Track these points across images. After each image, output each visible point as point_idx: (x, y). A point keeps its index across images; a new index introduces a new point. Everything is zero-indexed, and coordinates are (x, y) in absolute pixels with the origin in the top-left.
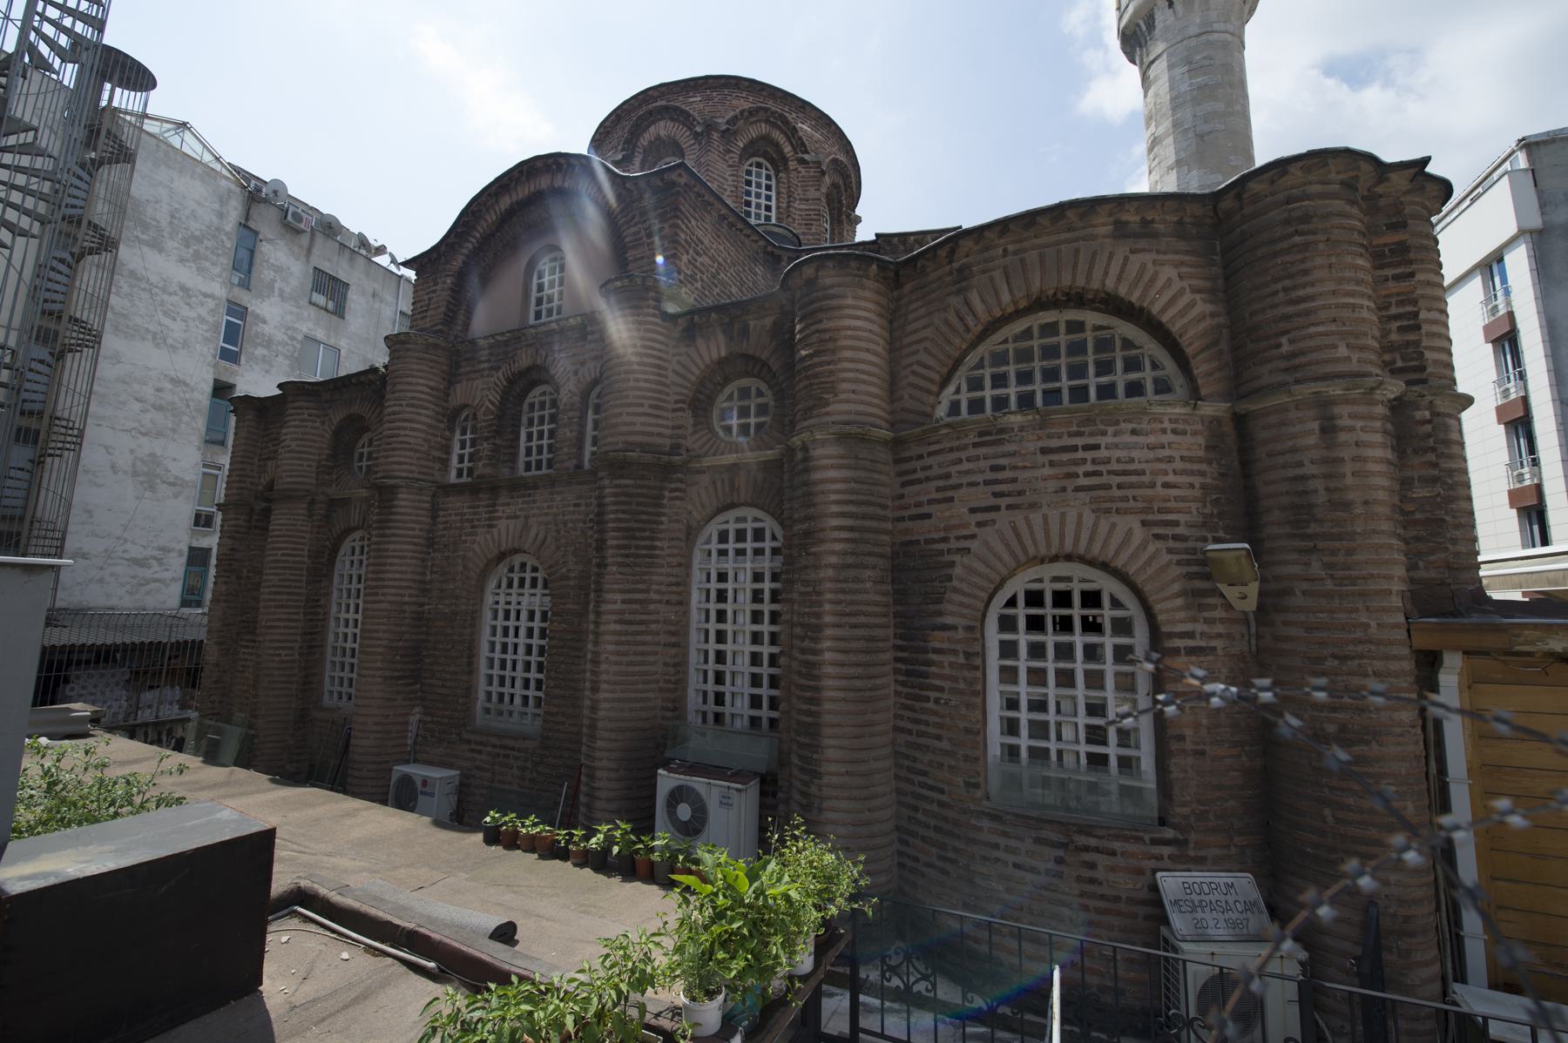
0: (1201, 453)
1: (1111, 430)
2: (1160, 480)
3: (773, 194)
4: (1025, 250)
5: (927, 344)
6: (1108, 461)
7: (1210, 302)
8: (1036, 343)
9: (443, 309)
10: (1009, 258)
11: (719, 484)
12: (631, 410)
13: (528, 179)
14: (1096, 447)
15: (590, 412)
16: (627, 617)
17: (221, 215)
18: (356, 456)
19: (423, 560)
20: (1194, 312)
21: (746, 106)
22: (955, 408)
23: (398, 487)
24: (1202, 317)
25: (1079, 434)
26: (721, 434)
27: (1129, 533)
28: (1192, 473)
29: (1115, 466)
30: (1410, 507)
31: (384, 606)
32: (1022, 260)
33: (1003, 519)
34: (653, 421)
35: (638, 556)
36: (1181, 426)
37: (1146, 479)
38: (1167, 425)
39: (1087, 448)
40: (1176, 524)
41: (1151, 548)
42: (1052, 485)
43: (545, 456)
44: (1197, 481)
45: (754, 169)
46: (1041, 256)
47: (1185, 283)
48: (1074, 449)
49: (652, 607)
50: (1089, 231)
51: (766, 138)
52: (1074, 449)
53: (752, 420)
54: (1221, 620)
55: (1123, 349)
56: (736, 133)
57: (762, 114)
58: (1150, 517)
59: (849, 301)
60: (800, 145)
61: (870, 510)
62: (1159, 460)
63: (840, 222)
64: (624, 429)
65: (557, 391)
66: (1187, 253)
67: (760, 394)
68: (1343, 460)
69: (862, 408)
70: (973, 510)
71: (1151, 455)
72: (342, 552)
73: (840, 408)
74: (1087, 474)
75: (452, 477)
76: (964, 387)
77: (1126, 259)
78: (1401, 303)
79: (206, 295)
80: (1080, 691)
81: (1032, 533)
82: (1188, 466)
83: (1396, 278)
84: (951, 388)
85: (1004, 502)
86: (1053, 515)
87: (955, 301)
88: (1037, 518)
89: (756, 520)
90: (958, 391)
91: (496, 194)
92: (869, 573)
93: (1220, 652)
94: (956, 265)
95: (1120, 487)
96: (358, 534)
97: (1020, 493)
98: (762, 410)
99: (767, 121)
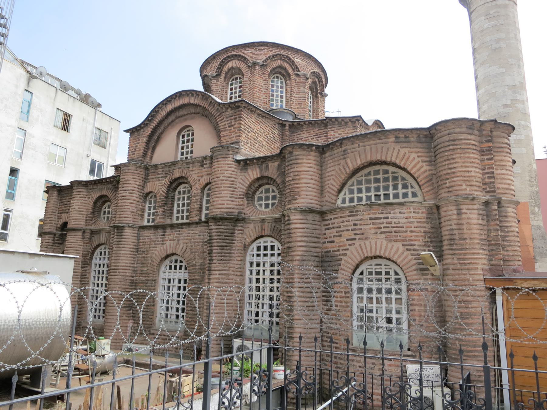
0: (425, 220)
1: (392, 212)
2: (409, 230)
3: (284, 90)
4: (365, 146)
5: (334, 177)
7: (429, 165)
9: (142, 151)
10: (360, 148)
11: (257, 228)
12: (222, 199)
13: (179, 99)
14: (387, 218)
15: (205, 197)
16: (221, 280)
17: (17, 86)
18: (102, 212)
19: (134, 258)
20: (422, 170)
22: (344, 201)
23: (123, 227)
24: (426, 171)
25: (382, 213)
26: (258, 207)
27: (398, 249)
28: (420, 227)
29: (393, 225)
30: (490, 239)
31: (119, 277)
32: (365, 149)
33: (357, 243)
34: (231, 203)
35: (225, 257)
36: (417, 211)
37: (404, 229)
38: (412, 210)
39: (385, 218)
40: (414, 245)
41: (405, 254)
42: (373, 231)
43: (185, 214)
44: (423, 230)
45: (275, 79)
46: (371, 149)
47: (420, 159)
48: (380, 218)
49: (231, 277)
50: (387, 140)
51: (281, 67)
52: (380, 218)
53: (270, 202)
54: (430, 279)
55: (401, 181)
56: (266, 65)
57: (279, 57)
58: (405, 243)
59: (305, 161)
60: (296, 68)
61: (313, 239)
62: (409, 223)
63: (317, 97)
64: (220, 206)
65: (191, 187)
66: (420, 148)
67: (273, 191)
68: (463, 224)
69: (309, 201)
70: (348, 240)
71: (406, 221)
72: (95, 254)
74: (384, 227)
75: (145, 223)
76: (347, 193)
77: (399, 150)
78: (489, 168)
79: (9, 126)
80: (384, 305)
81: (366, 248)
82: (419, 225)
83: (488, 159)
84: (342, 193)
85: (357, 237)
86: (373, 242)
87: (342, 162)
88: (367, 243)
89: (272, 242)
90: (345, 194)
91: (166, 104)
92: (311, 263)
93: (429, 290)
94: (343, 149)
95: (395, 232)
96: (103, 247)
97: (362, 234)
98: (274, 198)
99: (281, 59)
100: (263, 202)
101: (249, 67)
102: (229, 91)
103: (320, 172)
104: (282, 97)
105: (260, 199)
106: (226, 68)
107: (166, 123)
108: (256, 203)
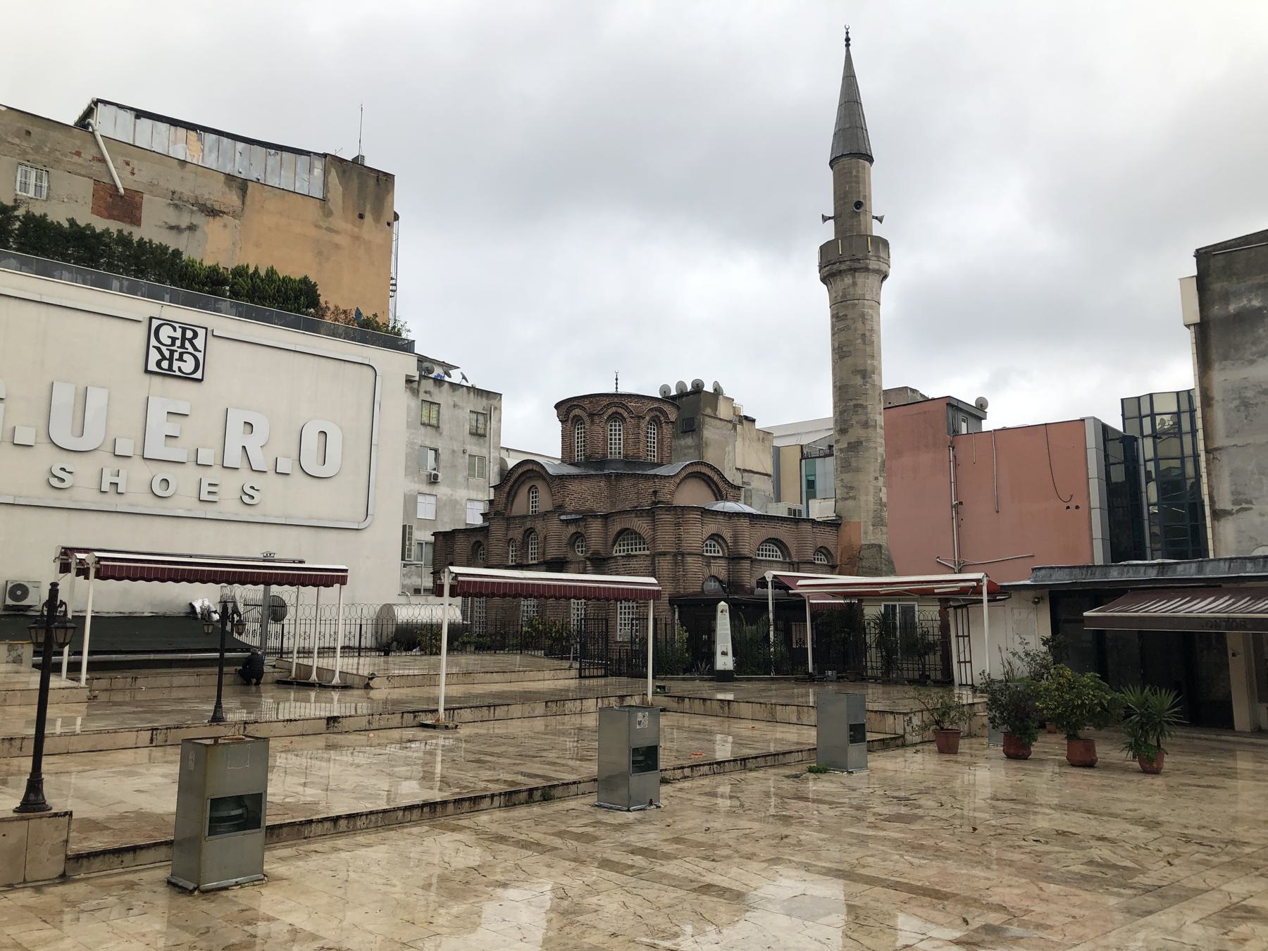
51: (616, 413)
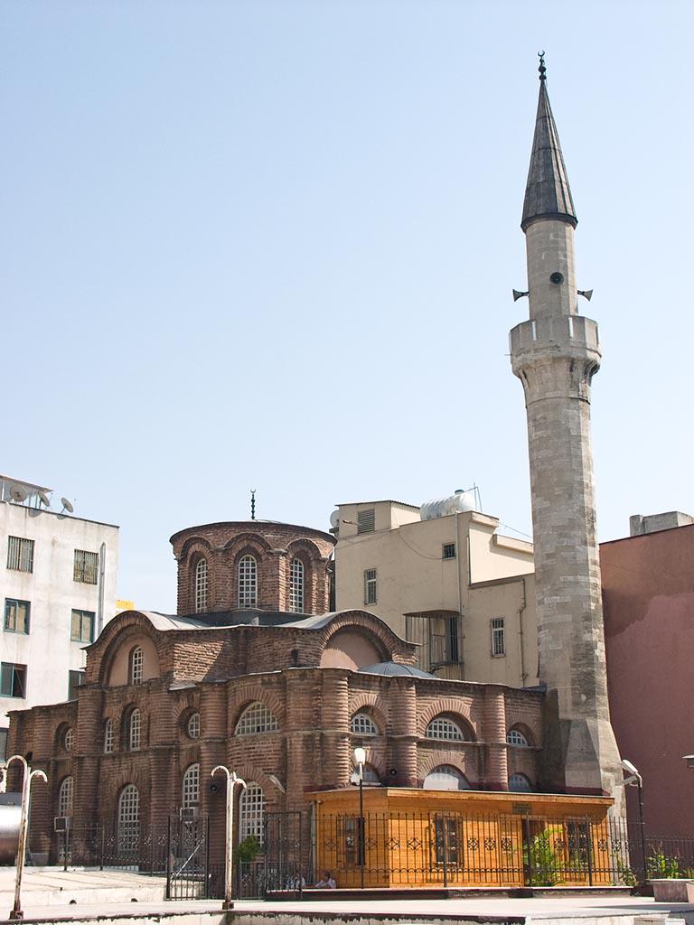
3: (256, 574)
6: (256, 752)
8: (255, 711)
21: (235, 535)
51: (248, 546)
73: (208, 734)
96: (68, 779)
100: (194, 730)
101: (212, 552)
102: (197, 579)
103: (224, 704)
104: (253, 583)
105: (192, 728)
106: (190, 553)
107: (118, 642)
108: (190, 731)
